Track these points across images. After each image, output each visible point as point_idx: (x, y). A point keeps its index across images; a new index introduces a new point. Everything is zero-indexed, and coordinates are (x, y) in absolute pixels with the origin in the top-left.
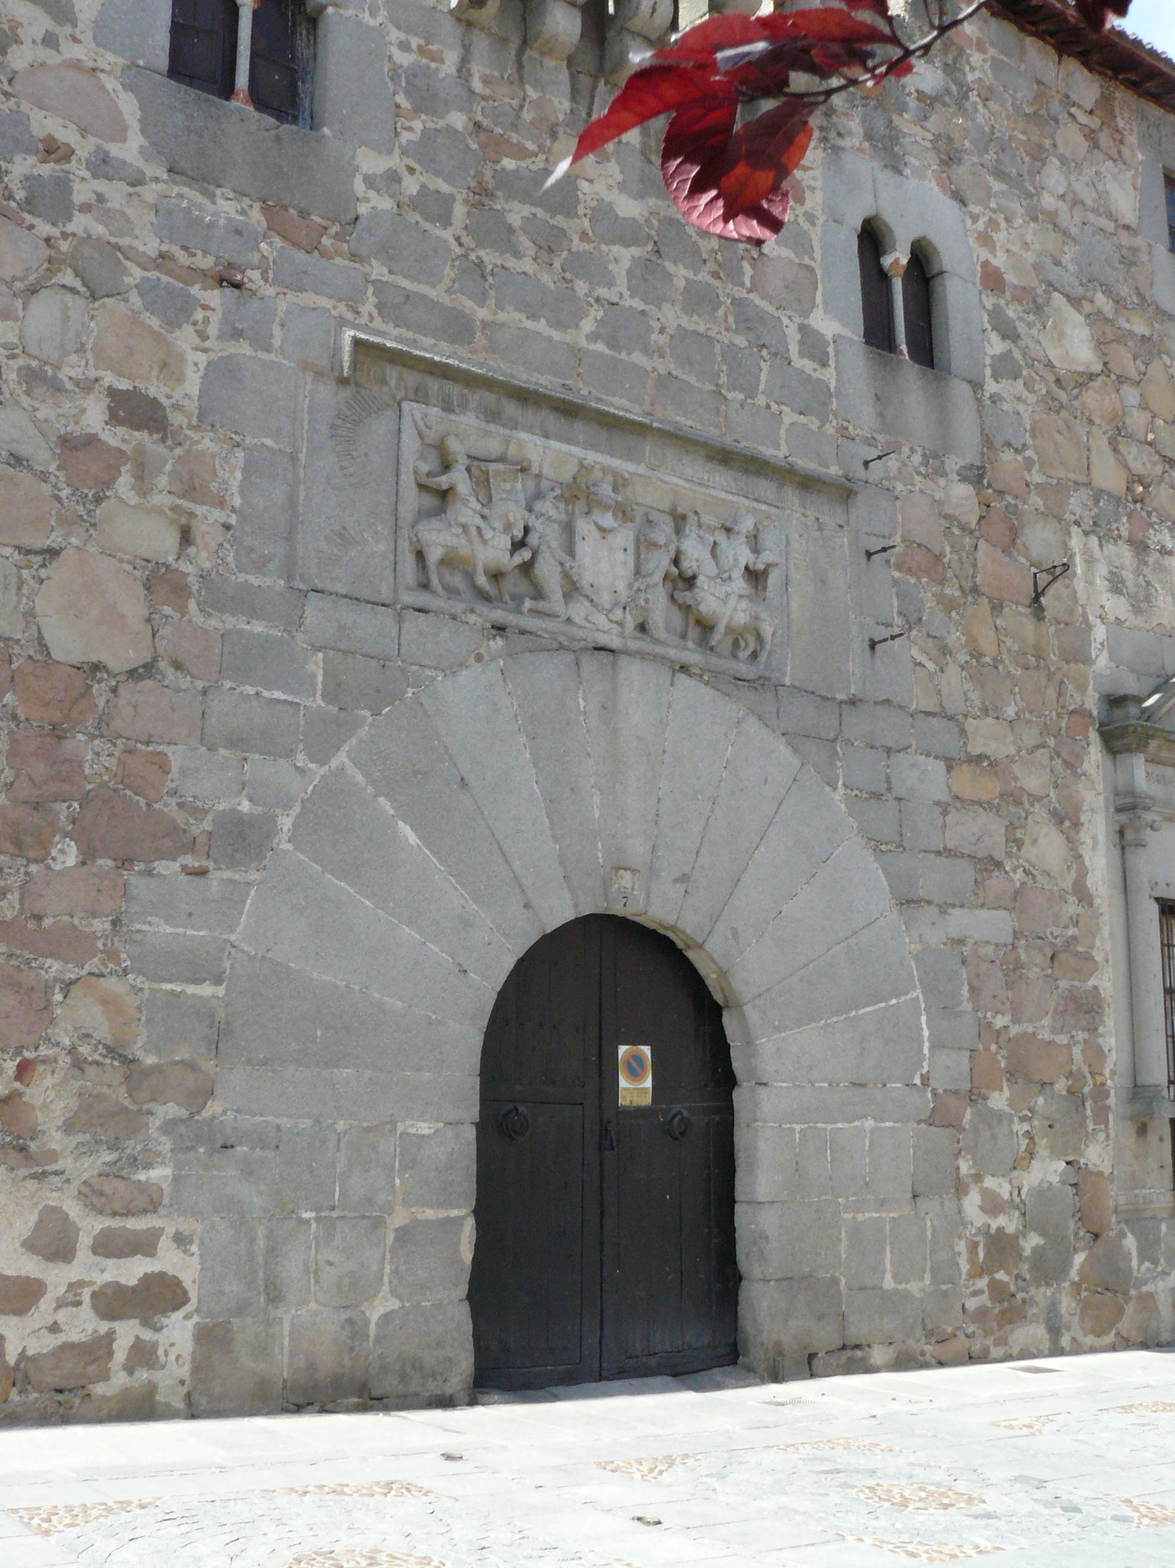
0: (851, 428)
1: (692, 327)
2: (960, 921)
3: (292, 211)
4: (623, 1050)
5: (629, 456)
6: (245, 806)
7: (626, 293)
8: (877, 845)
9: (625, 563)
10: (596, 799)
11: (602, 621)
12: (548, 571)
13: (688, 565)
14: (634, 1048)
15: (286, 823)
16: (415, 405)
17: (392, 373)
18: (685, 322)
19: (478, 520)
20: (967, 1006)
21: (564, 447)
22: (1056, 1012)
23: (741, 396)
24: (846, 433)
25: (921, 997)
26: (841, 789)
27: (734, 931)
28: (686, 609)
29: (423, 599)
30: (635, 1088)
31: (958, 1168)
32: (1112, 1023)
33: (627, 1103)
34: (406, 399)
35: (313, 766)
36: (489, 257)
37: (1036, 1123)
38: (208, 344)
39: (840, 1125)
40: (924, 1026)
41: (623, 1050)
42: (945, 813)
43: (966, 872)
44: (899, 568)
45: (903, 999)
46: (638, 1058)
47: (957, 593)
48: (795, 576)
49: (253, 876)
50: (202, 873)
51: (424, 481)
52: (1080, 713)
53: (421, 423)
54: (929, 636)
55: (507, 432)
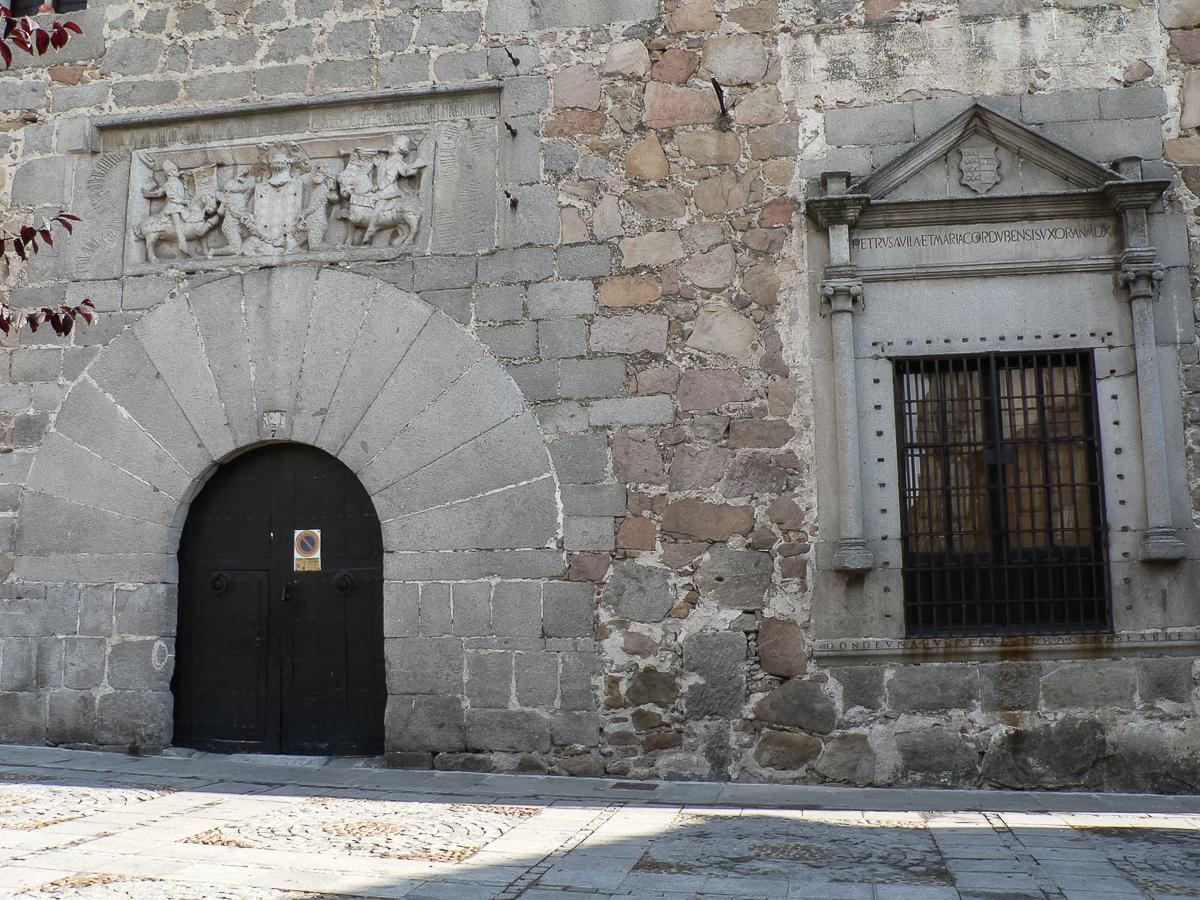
0: (501, 38)
1: (351, 19)
2: (601, 412)
3: (66, 64)
4: (297, 533)
5: (294, 129)
6: (31, 412)
7: (293, 18)
8: (509, 364)
9: (294, 204)
10: (253, 369)
11: (269, 249)
12: (230, 227)
13: (346, 189)
14: (307, 531)
15: (53, 417)
16: (140, 151)
17: (126, 136)
18: (345, 18)
19: (180, 208)
20: (611, 481)
21: (245, 141)
22: (731, 477)
23: (390, 53)
24: (496, 44)
25: (555, 477)
26: (473, 324)
27: (364, 445)
28: (345, 220)
29: (145, 268)
30: (307, 557)
31: (598, 616)
32: (814, 482)
33: (301, 569)
34: (135, 149)
35: (68, 383)
36: (186, 38)
37: (698, 577)
38: (17, 161)
39: (464, 581)
40: (558, 500)
41: (297, 533)
42: (591, 321)
43: (617, 368)
44: (547, 134)
45: (535, 479)
46: (311, 539)
47: (618, 135)
48: (440, 168)
49: (35, 449)
50: (10, 451)
51: (152, 194)
52: (785, 204)
53: (145, 160)
54: (581, 179)
55: (203, 146)
